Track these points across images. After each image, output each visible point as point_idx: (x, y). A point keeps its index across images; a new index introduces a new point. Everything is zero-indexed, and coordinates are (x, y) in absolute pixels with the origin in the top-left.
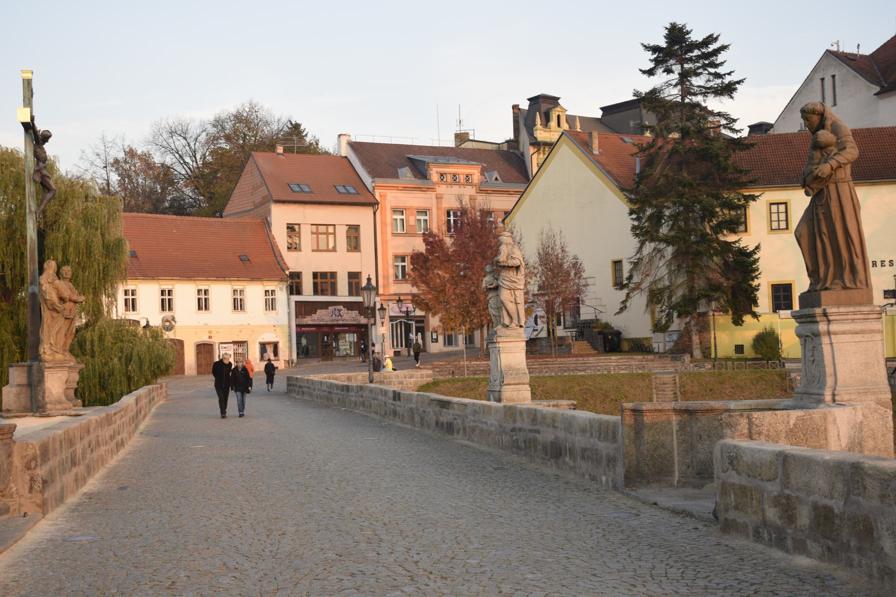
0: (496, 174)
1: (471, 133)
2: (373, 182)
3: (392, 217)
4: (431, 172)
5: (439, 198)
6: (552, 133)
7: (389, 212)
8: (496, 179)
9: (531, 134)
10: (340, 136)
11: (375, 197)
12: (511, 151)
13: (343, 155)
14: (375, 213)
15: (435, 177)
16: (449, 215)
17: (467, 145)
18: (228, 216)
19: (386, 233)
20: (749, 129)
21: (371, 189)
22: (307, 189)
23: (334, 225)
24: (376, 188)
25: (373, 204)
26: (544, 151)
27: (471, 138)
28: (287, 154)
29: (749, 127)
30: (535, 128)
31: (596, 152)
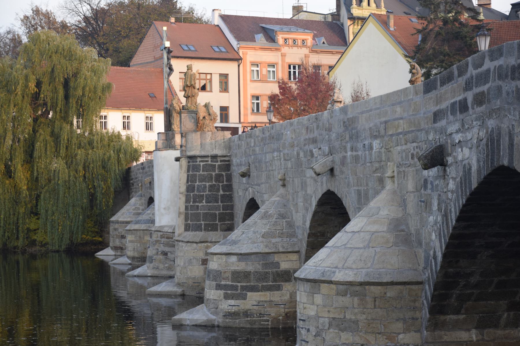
0: (323, 39)
1: (304, 6)
2: (238, 44)
3: (250, 68)
4: (278, 37)
5: (283, 56)
6: (364, 10)
7: (248, 64)
8: (324, 43)
9: (349, 11)
10: (213, 10)
11: (239, 55)
12: (334, 22)
13: (216, 24)
14: (239, 66)
15: (281, 41)
16: (290, 68)
17: (302, 16)
18: (134, 65)
19: (246, 80)
20: (511, 6)
21: (236, 49)
22: (193, 49)
23: (211, 74)
24: (240, 48)
25: (238, 60)
26: (358, 23)
27: (304, 9)
28: (177, 23)
29: (512, 5)
30: (351, 7)
31: (392, 29)
